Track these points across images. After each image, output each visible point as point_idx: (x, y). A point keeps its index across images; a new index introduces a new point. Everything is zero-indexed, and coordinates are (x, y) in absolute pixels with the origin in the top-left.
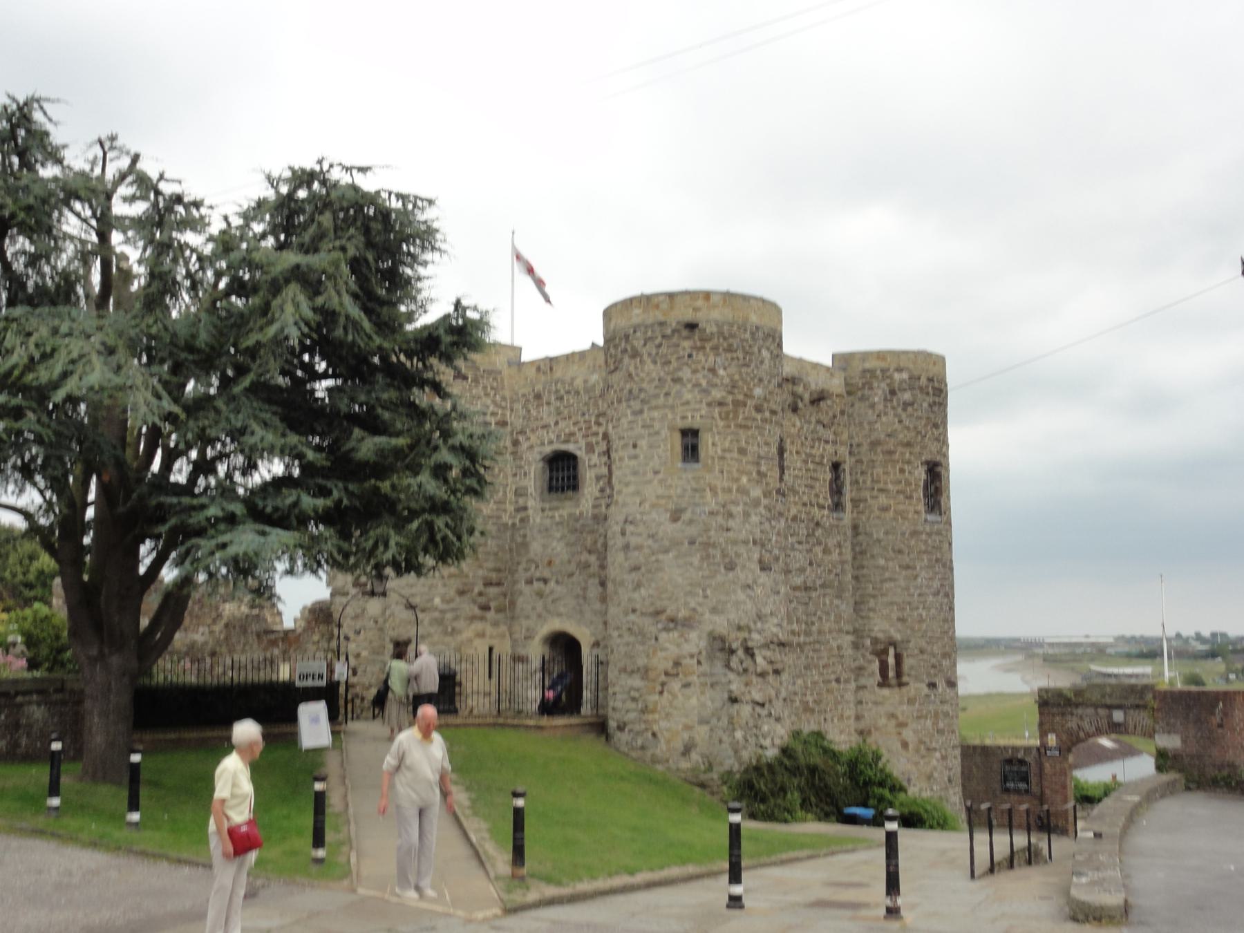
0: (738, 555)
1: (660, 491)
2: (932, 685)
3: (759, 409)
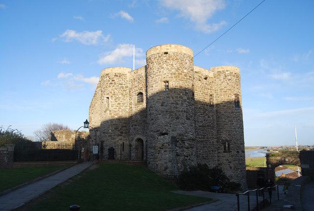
0: (180, 115)
2: (238, 152)
3: (185, 75)
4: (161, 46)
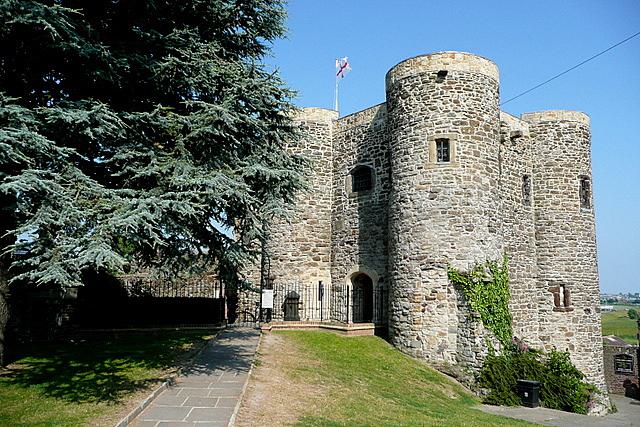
0: (475, 221)
4: (429, 56)
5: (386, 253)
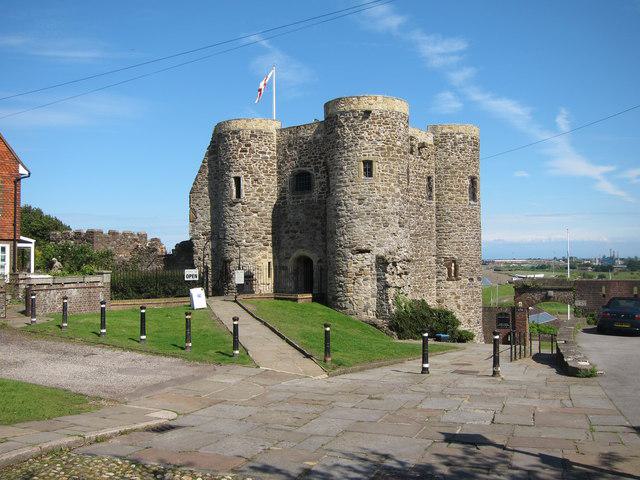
0: (389, 220)
1: (353, 190)
2: (471, 280)
5: (325, 240)
